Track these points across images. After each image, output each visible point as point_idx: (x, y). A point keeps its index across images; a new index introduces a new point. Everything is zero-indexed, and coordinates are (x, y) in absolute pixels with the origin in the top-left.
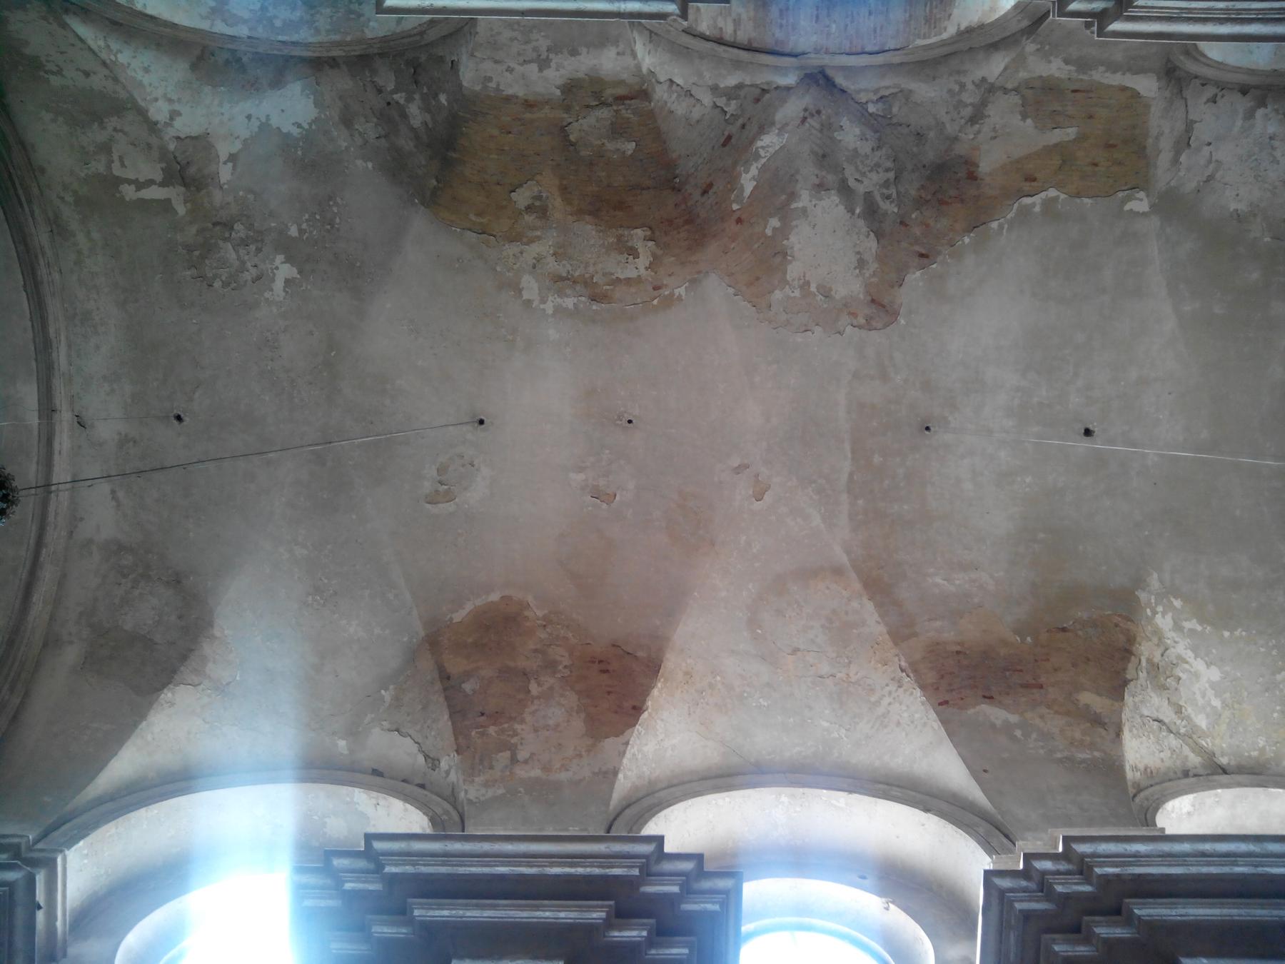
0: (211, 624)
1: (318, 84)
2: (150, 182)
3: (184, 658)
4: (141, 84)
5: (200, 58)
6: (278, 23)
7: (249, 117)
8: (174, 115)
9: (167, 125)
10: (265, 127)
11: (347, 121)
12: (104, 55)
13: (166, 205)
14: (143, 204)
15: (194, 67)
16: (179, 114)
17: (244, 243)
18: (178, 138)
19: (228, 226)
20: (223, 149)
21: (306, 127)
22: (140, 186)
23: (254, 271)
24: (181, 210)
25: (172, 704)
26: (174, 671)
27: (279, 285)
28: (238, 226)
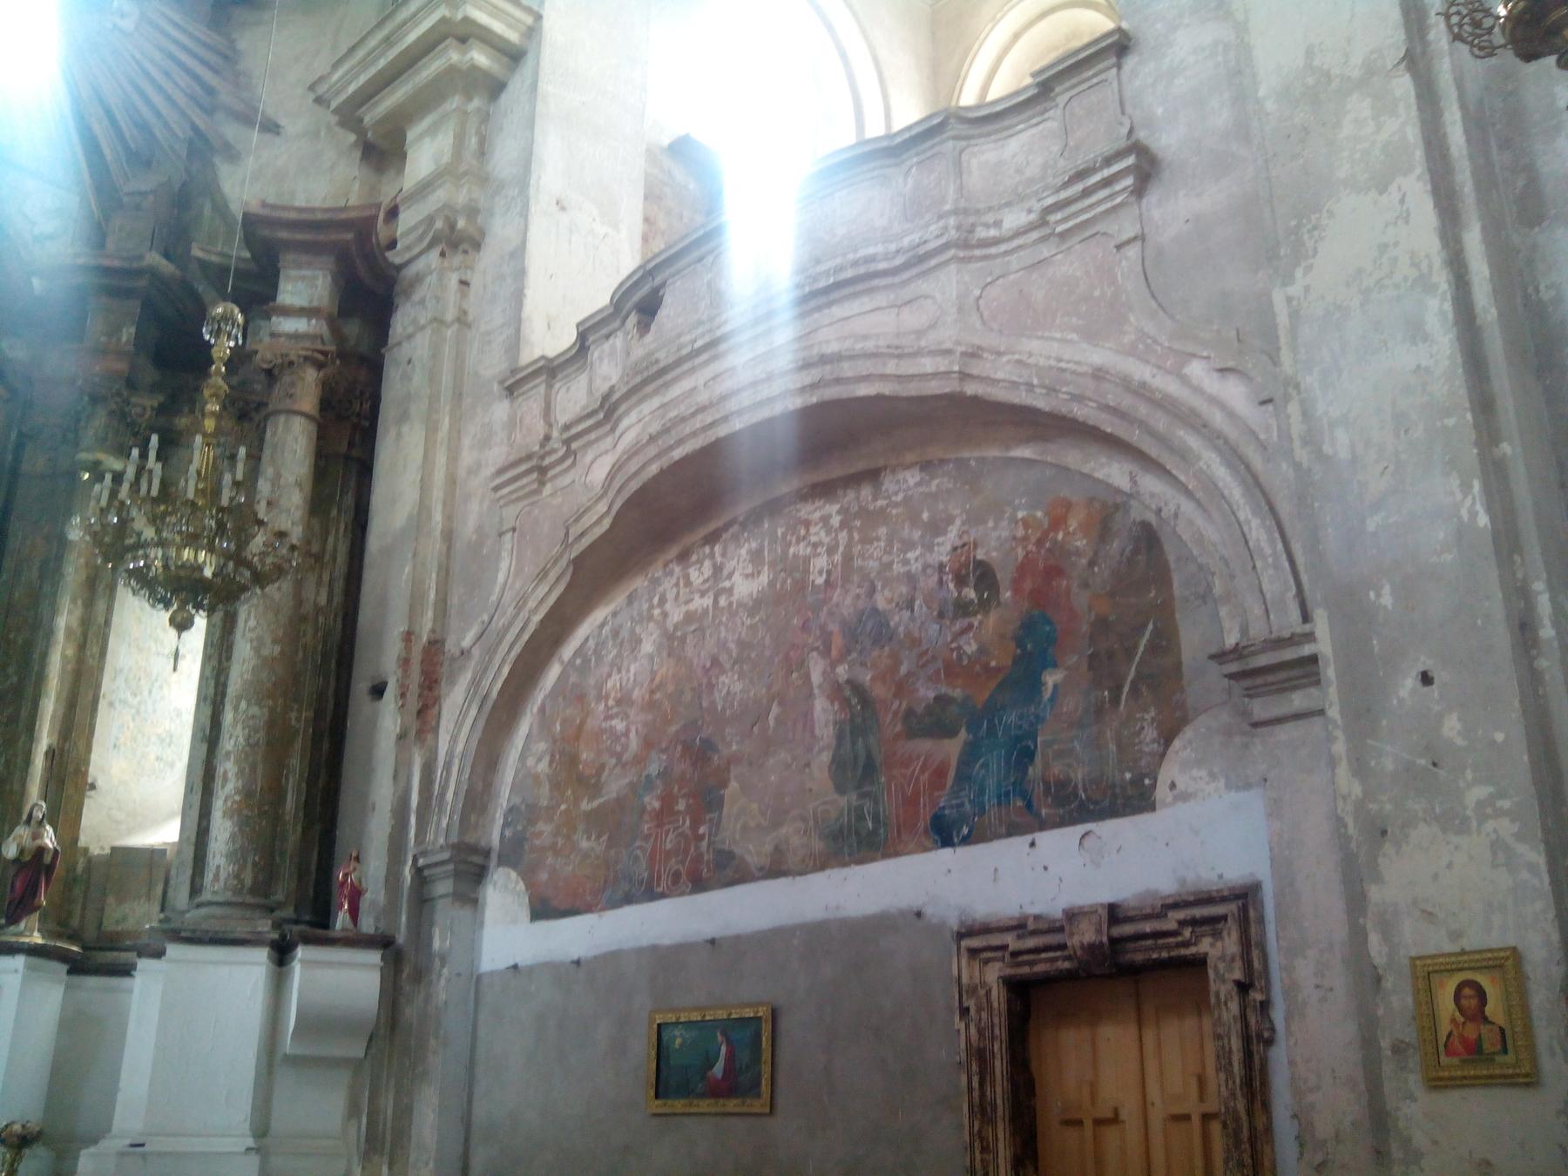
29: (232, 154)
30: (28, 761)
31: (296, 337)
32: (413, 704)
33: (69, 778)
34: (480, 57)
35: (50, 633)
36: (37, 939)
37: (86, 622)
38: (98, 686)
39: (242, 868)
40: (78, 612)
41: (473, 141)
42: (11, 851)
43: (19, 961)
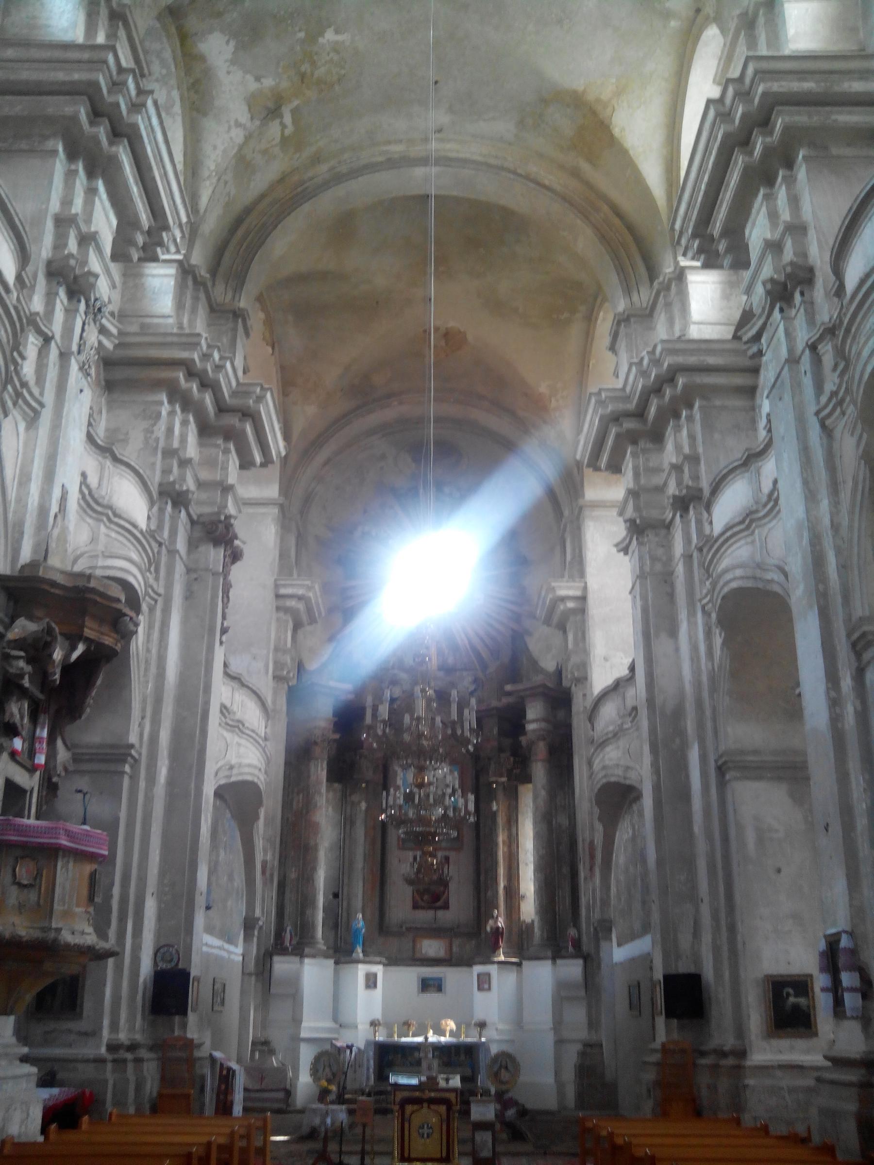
0: (575, 92)
1: (196, 34)
2: (282, 123)
3: (594, 113)
4: (225, 151)
5: (198, 110)
6: (164, 72)
7: (228, 73)
8: (238, 124)
9: (245, 128)
10: (233, 62)
11: (219, 15)
12: (214, 180)
13: (295, 112)
14: (295, 121)
15: (205, 114)
16: (236, 121)
17: (313, 64)
18: (252, 119)
19: (303, 76)
20: (253, 86)
21: (227, 37)
22: (284, 126)
23: (332, 55)
24: (296, 103)
25: (623, 130)
26: (602, 123)
27: (339, 38)
28: (303, 69)
29: (530, 634)
30: (497, 892)
31: (534, 731)
32: (588, 866)
33: (513, 894)
34: (571, 605)
35: (497, 844)
36: (502, 958)
37: (510, 836)
38: (518, 860)
39: (543, 932)
40: (506, 834)
41: (580, 634)
42: (488, 929)
43: (495, 966)
